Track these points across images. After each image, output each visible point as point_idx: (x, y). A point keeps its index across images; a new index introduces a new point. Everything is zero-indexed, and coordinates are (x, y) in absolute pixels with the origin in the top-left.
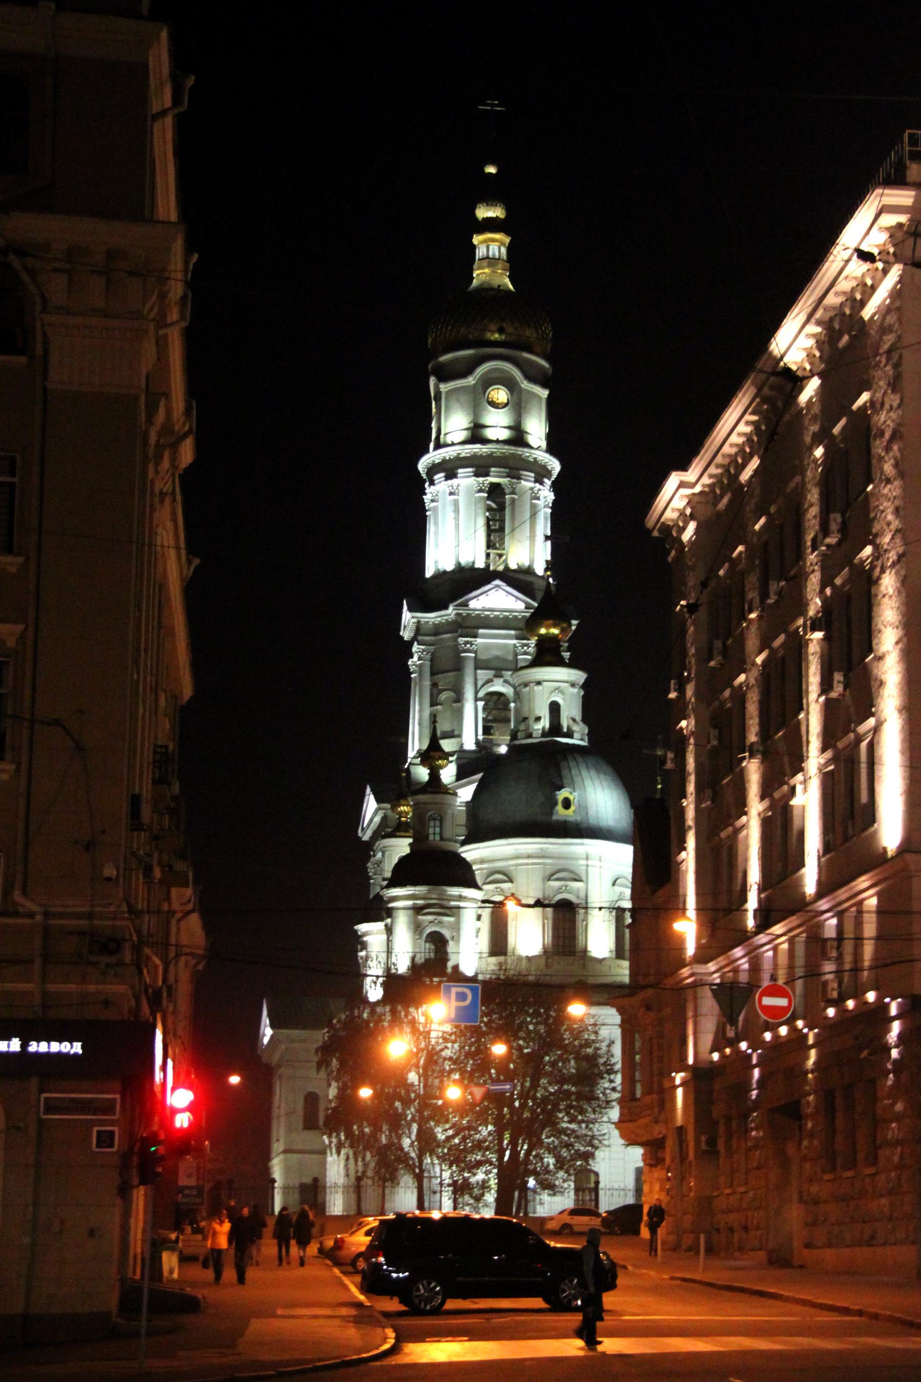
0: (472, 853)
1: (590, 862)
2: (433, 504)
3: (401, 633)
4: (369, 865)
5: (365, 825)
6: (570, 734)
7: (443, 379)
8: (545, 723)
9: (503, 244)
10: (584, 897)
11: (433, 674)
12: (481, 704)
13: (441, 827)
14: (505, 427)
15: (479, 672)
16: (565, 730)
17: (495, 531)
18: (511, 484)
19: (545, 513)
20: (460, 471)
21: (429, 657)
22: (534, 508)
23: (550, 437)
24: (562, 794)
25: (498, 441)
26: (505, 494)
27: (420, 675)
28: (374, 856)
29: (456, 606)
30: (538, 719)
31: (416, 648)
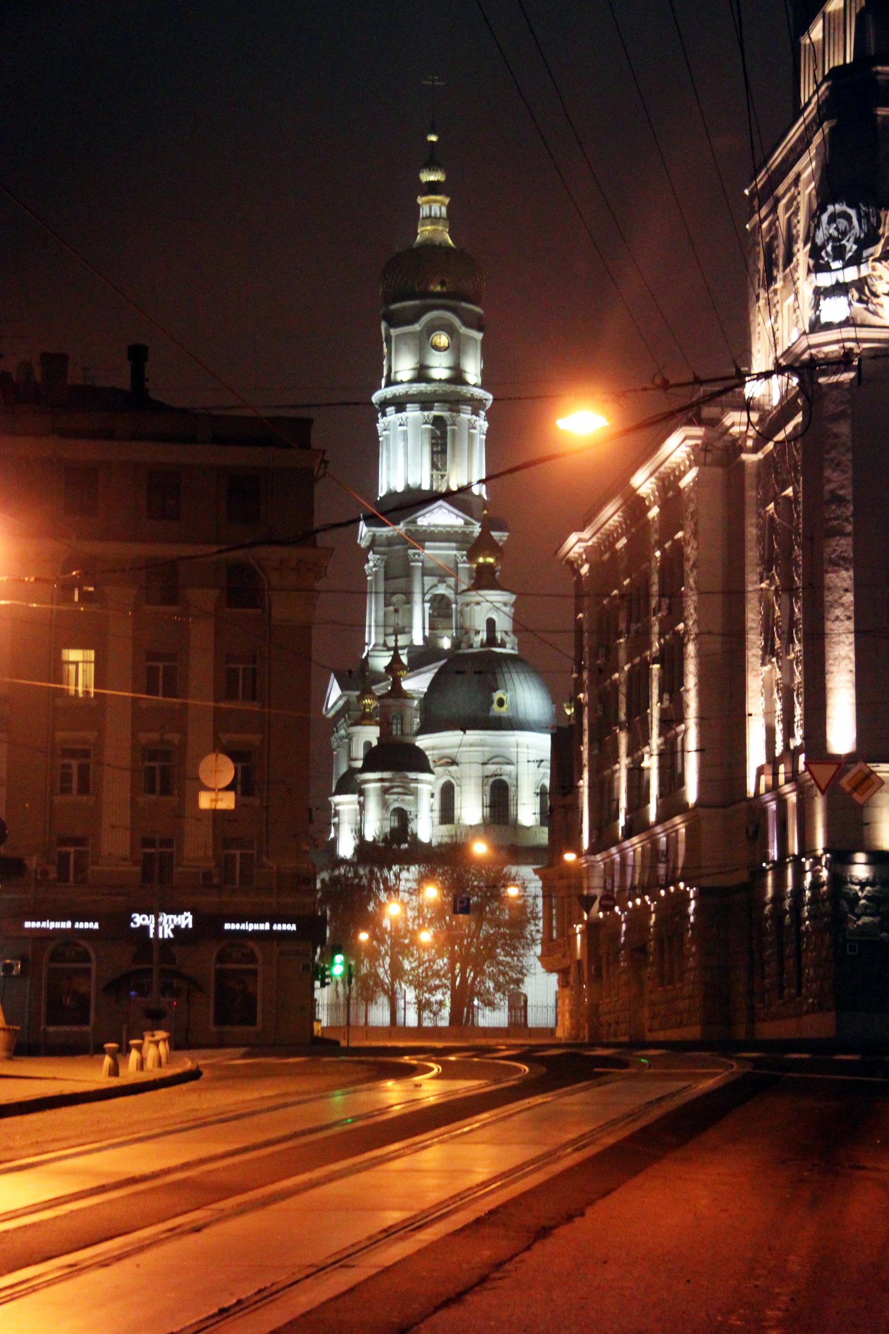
0: (423, 742)
1: (519, 750)
2: (385, 433)
3: (358, 541)
4: (333, 739)
5: (330, 706)
6: (503, 645)
7: (392, 324)
8: (483, 636)
9: (442, 203)
10: (515, 777)
11: (386, 579)
12: (427, 605)
13: (402, 724)
14: (447, 368)
15: (426, 578)
16: (499, 641)
17: (437, 452)
18: (452, 417)
19: (481, 439)
20: (408, 405)
21: (383, 565)
22: (471, 437)
23: (484, 373)
24: (497, 695)
25: (440, 381)
26: (446, 425)
27: (376, 579)
28: (337, 732)
29: (408, 522)
30: (477, 632)
31: (371, 556)
